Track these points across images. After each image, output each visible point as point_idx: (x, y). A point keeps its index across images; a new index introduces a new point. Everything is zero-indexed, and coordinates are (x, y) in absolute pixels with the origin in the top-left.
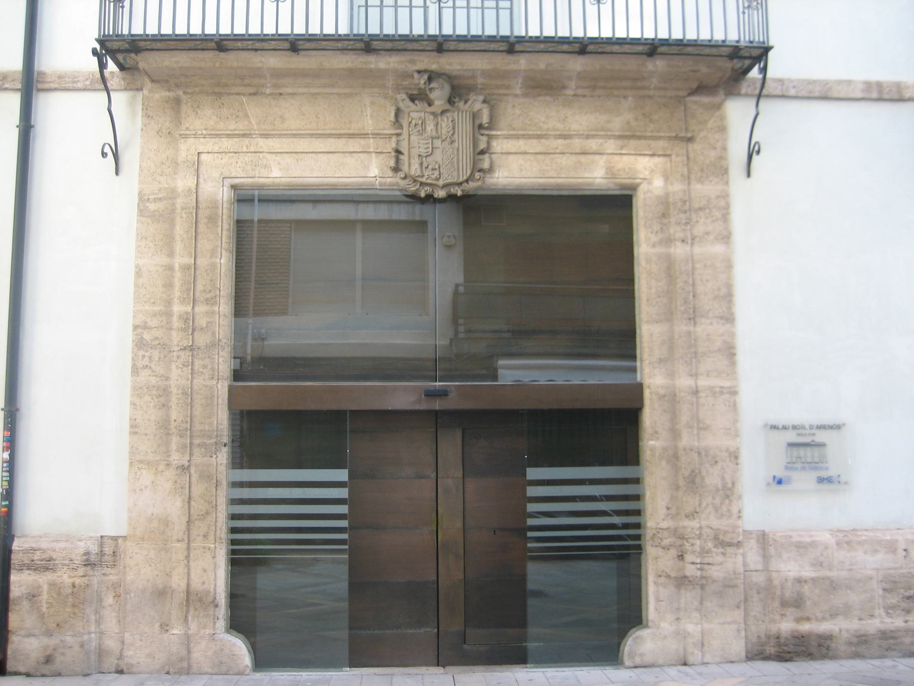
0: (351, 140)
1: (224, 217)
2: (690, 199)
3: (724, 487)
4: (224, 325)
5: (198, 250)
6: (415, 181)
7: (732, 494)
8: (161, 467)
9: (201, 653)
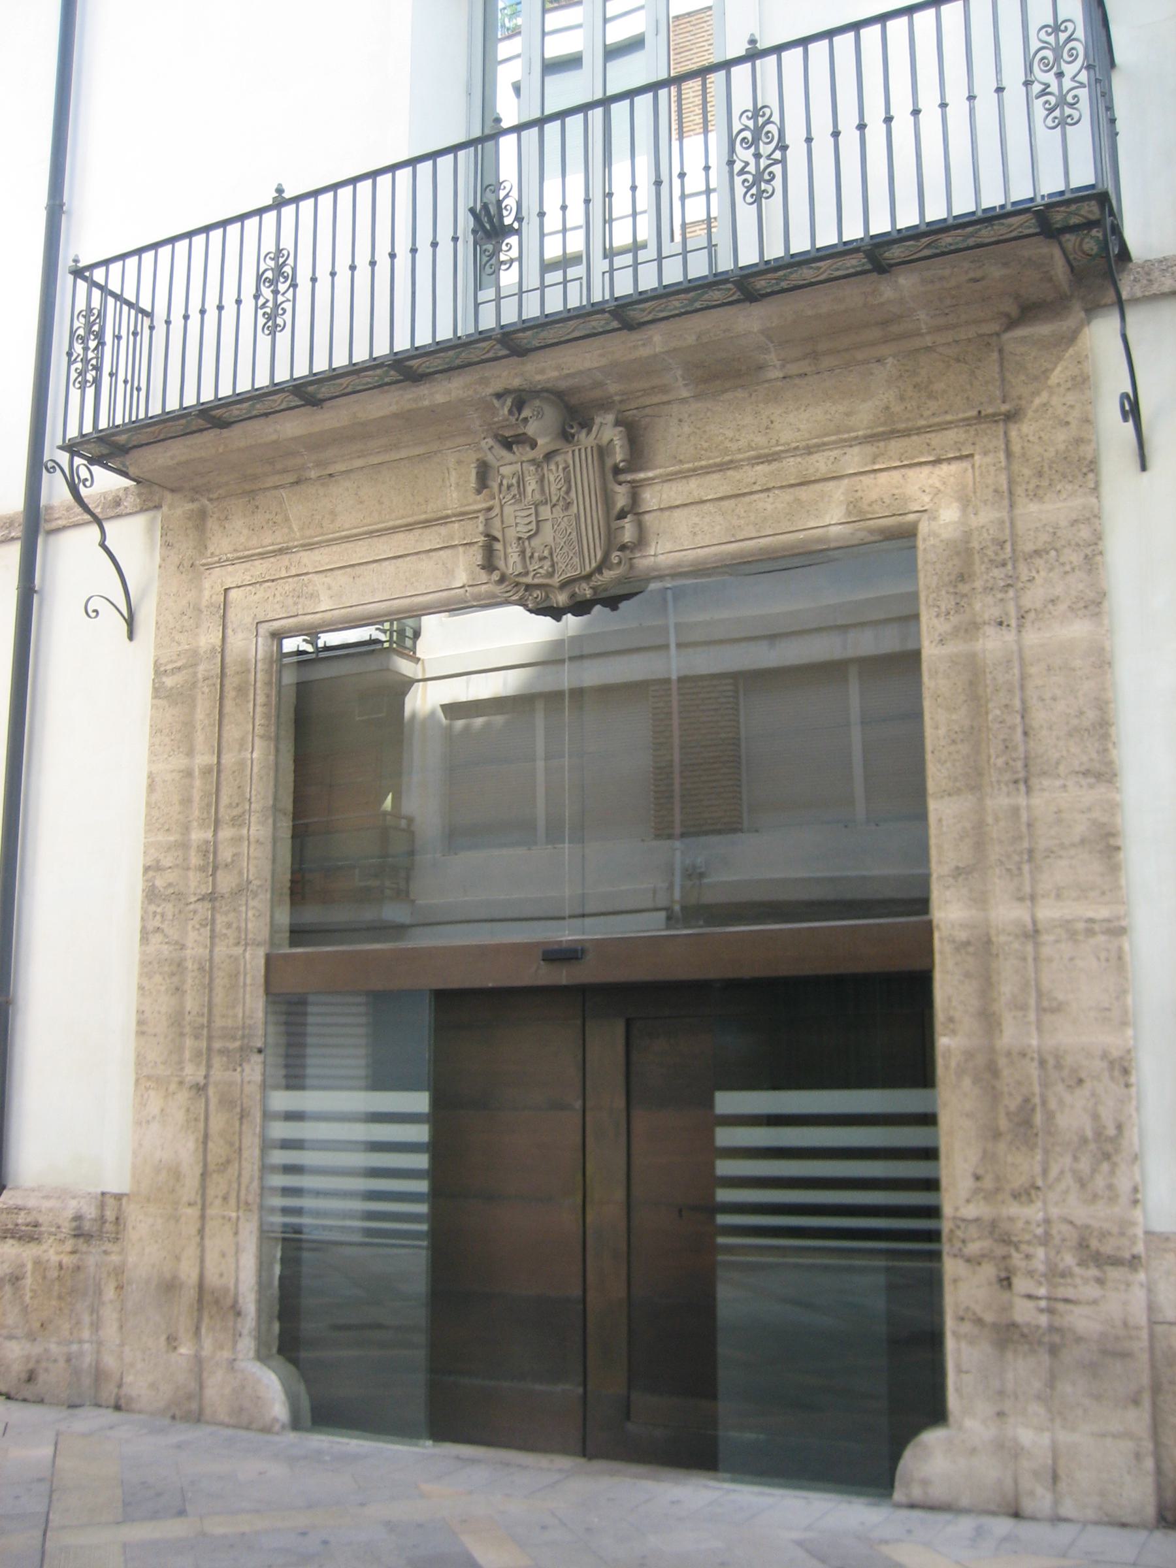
0: (428, 531)
1: (259, 684)
2: (1013, 534)
3: (1099, 1134)
4: (256, 858)
5: (224, 740)
6: (517, 584)
7: (1117, 1151)
8: (173, 1087)
9: (217, 1389)
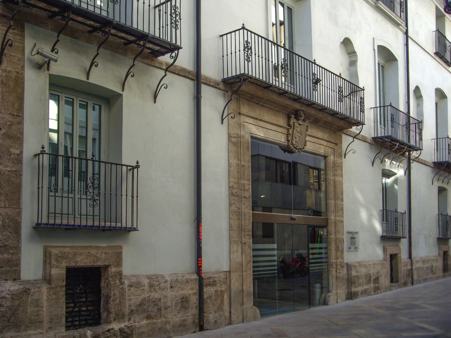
8: (239, 243)
